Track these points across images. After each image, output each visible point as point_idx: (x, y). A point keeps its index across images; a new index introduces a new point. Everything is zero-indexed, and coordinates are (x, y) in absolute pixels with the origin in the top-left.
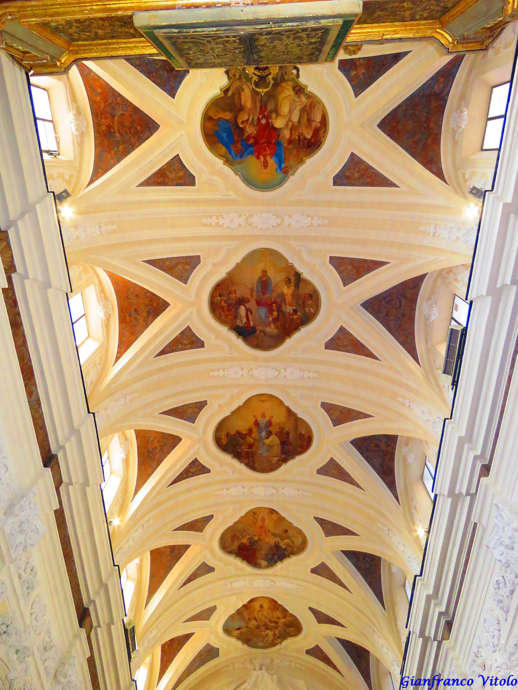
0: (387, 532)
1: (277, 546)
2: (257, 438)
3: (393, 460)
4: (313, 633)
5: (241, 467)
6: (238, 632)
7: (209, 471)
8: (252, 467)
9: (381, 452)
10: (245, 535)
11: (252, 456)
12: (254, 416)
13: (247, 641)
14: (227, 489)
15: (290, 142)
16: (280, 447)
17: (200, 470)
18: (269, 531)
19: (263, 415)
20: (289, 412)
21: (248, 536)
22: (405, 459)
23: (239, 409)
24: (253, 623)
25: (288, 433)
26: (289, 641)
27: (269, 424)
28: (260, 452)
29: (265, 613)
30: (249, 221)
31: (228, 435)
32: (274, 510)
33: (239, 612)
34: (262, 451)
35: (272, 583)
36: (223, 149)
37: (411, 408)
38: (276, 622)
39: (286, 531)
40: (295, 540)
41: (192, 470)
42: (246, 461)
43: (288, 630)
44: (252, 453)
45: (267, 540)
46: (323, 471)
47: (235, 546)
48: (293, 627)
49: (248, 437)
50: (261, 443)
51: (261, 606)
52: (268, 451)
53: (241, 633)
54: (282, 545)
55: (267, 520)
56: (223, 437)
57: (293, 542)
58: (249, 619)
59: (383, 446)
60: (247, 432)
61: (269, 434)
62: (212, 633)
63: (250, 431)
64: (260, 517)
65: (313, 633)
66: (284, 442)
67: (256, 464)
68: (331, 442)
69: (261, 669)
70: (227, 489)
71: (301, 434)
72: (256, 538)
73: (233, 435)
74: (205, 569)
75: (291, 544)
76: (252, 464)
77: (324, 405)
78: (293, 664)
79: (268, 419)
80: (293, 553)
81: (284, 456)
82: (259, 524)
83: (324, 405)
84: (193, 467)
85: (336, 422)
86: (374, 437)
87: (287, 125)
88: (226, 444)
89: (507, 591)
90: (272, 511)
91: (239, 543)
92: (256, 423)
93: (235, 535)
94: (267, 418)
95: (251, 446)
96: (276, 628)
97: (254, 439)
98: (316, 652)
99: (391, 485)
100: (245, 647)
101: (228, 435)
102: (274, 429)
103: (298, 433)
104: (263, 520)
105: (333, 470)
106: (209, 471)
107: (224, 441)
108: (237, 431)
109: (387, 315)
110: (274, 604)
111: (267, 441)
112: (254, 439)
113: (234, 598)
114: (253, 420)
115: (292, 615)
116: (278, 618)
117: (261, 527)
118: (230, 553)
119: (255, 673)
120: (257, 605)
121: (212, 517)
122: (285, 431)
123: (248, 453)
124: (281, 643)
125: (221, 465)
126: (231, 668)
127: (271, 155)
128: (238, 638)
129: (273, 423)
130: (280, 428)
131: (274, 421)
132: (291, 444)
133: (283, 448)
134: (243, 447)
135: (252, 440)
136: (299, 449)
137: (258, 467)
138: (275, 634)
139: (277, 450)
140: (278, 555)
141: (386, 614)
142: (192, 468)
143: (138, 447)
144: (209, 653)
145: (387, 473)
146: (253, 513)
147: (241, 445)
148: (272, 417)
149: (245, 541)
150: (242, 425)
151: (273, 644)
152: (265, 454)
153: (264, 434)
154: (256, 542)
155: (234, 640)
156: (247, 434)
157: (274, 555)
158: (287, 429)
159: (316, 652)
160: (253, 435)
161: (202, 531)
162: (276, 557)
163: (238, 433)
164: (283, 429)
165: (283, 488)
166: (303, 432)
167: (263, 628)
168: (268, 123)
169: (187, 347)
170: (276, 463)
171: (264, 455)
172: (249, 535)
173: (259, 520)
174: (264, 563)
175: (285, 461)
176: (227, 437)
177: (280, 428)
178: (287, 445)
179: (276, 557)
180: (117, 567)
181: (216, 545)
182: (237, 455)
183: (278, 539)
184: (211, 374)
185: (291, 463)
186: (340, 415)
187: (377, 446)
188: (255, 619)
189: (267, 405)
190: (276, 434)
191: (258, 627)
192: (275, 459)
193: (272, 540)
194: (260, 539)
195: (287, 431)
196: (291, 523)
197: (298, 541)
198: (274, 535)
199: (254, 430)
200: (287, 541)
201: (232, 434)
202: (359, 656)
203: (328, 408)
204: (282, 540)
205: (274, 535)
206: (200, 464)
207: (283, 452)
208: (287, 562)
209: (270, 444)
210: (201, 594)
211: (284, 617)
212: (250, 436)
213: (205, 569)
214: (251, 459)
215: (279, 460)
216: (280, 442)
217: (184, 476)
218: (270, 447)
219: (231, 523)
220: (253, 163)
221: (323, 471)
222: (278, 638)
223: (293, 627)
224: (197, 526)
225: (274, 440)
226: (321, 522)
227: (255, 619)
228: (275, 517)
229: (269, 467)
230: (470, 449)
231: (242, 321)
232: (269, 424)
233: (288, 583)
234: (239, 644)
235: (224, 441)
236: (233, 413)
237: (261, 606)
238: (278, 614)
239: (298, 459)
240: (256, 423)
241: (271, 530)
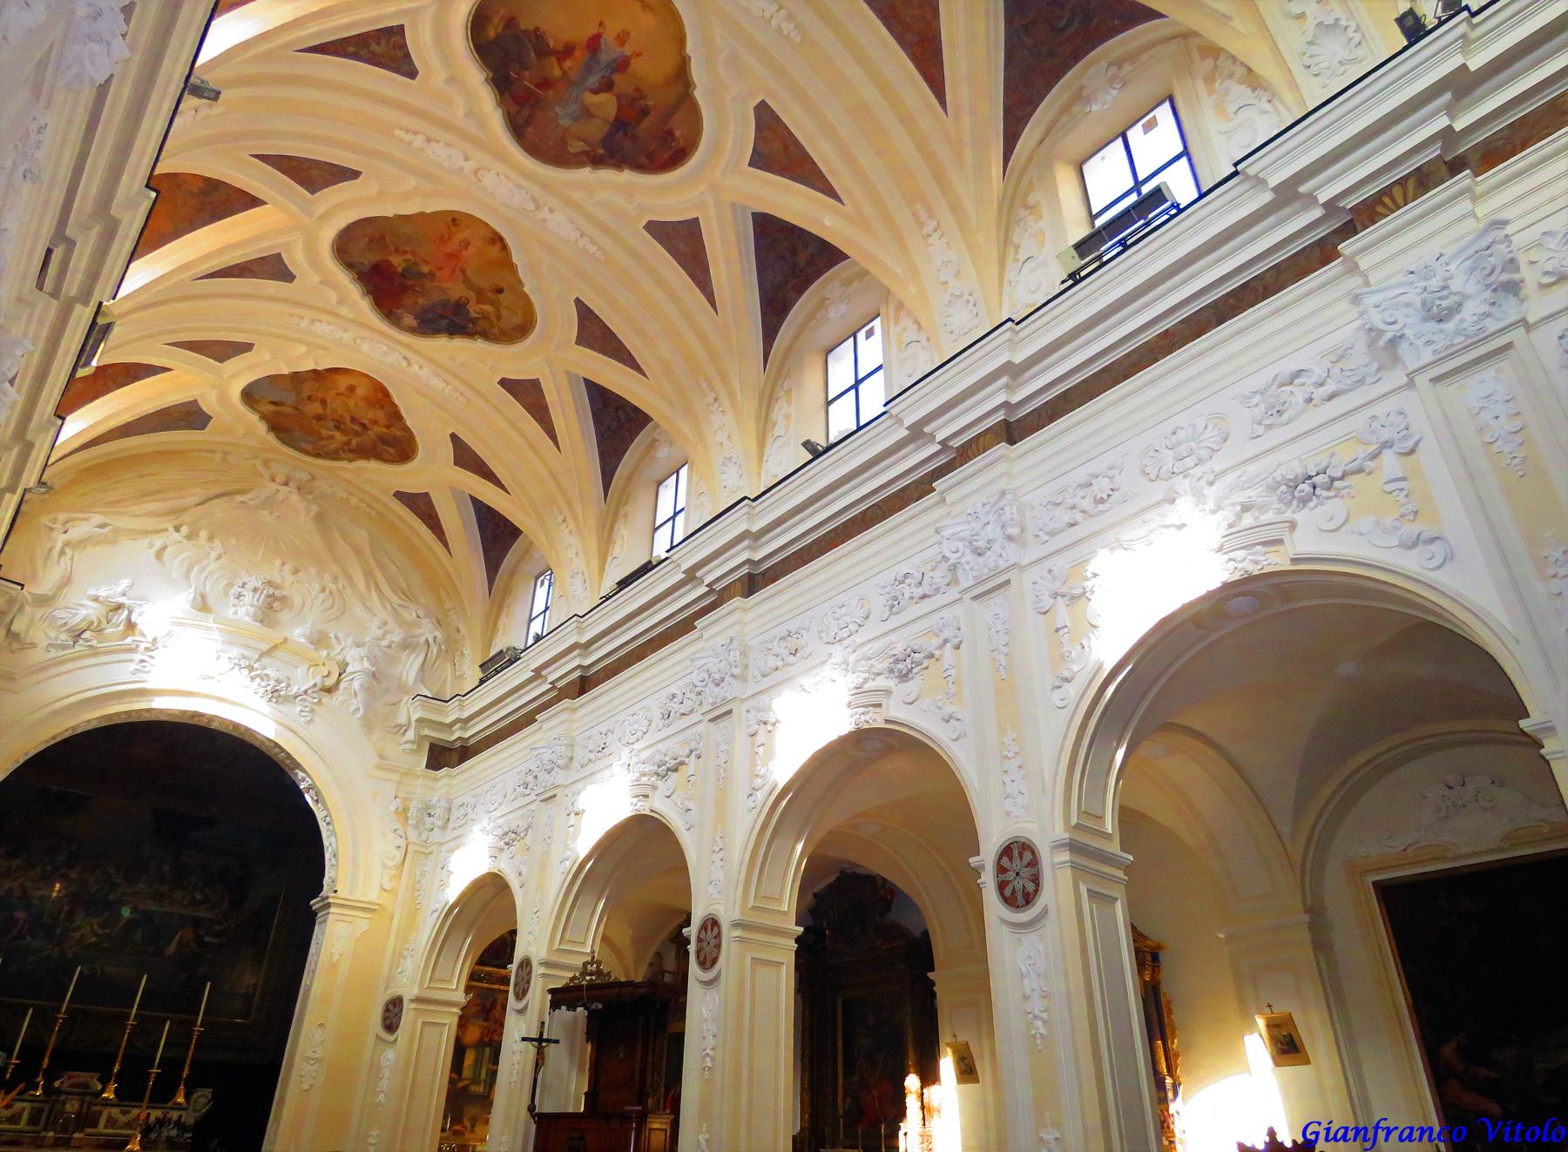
0: (711, 400)
1: (460, 306)
2: (573, 75)
3: (800, 291)
4: (431, 470)
6: (272, 408)
7: (412, 73)
8: (518, 129)
9: (792, 265)
12: (601, 24)
13: (277, 426)
14: (429, 140)
16: (607, 127)
18: (463, 271)
19: (622, 38)
20: (681, 75)
21: (409, 257)
22: (822, 304)
24: (316, 408)
25: (645, 112)
26: (373, 465)
27: (622, 65)
28: (558, 110)
29: (352, 403)
31: (511, 23)
32: (501, 239)
33: (296, 377)
34: (563, 115)
35: (404, 363)
37: (931, 240)
38: (363, 425)
39: (500, 291)
40: (505, 313)
41: (374, 47)
42: (514, 109)
43: (381, 447)
45: (445, 285)
46: (660, 231)
47: (368, 259)
48: (399, 447)
49: (554, 60)
51: (352, 389)
52: (576, 119)
53: (276, 413)
54: (474, 310)
56: (496, 20)
57: (499, 317)
58: (309, 398)
59: (802, 259)
60: (560, 48)
61: (607, 86)
62: (220, 387)
63: (567, 51)
64: (461, 236)
65: (431, 470)
66: (622, 125)
67: (530, 129)
68: (720, 186)
69: (286, 484)
70: (429, 140)
71: (670, 133)
72: (425, 269)
73: (524, 32)
74: (273, 268)
75: (494, 319)
77: (762, 109)
78: (354, 501)
80: (486, 336)
81: (601, 151)
82: (452, 246)
83: (762, 109)
84: (383, 42)
85: (761, 160)
86: (801, 233)
89: (919, 592)
90: (497, 240)
91: (379, 257)
92: (594, 43)
93: (382, 237)
94: (627, 50)
95: (545, 84)
96: (357, 434)
97: (565, 72)
98: (421, 505)
99: (770, 334)
100: (272, 439)
102: (622, 83)
103: (667, 128)
104: (466, 244)
105: (683, 241)
106: (412, 73)
107: (492, 32)
108: (537, 29)
109: (1026, 28)
110: (381, 396)
112: (565, 72)
113: (302, 349)
114: (592, 30)
115: (408, 430)
116: (375, 422)
117: (451, 256)
118: (349, 265)
119: (274, 486)
120: (343, 382)
121: (355, 174)
124: (351, 461)
125: (452, 80)
126: (218, 457)
128: (263, 417)
129: (629, 71)
130: (638, 90)
131: (635, 64)
132: (634, 138)
133: (611, 134)
134: (527, 74)
135: (557, 72)
136: (644, 160)
138: (348, 443)
139: (596, 129)
140: (450, 320)
141: (604, 507)
142: (378, 44)
144: (190, 416)
145: (775, 309)
146: (455, 220)
147: (525, 67)
148: (639, 55)
149: (397, 262)
151: (333, 455)
152: (565, 122)
153: (593, 80)
154: (422, 275)
155: (254, 418)
156: (553, 52)
157: (442, 317)
158: (650, 103)
159: (421, 505)
160: (568, 64)
161: (312, 192)
162: (444, 322)
163: (538, 36)
164: (643, 97)
165: (551, 211)
166: (678, 133)
167: (331, 425)
170: (576, 155)
172: (414, 253)
174: (409, 320)
175: (597, 162)
178: (626, 135)
179: (444, 322)
180: (154, 194)
181: (329, 234)
182: (501, 83)
183: (472, 295)
185: (608, 175)
186: (778, 150)
187: (794, 251)
188: (324, 402)
189: (648, 20)
190: (619, 97)
191: (319, 418)
192: (576, 146)
193: (456, 291)
194: (432, 275)
195: (647, 107)
196: (520, 282)
197: (511, 319)
198: (467, 282)
199: (578, 53)
200: (488, 308)
201: (523, 26)
202: (498, 535)
203: (767, 120)
204: (479, 302)
205: (467, 282)
206: (403, 46)
207: (607, 142)
208: (459, 344)
210: (229, 311)
211: (388, 427)
212: (560, 60)
213: (273, 268)
214: (526, 113)
215: (585, 153)
217: (351, 49)
218: (587, 113)
219: (389, 210)
221: (660, 231)
222: (351, 451)
223: (399, 447)
224: (311, 175)
225: (606, 104)
226: (586, 315)
227: (324, 402)
228: (495, 251)
229: (552, 151)
230: (1007, 386)
232: (622, 65)
233: (436, 380)
234: (262, 428)
235: (492, 32)
237: (352, 389)
238: (380, 415)
239: (627, 176)
240: (594, 43)
241: (470, 273)
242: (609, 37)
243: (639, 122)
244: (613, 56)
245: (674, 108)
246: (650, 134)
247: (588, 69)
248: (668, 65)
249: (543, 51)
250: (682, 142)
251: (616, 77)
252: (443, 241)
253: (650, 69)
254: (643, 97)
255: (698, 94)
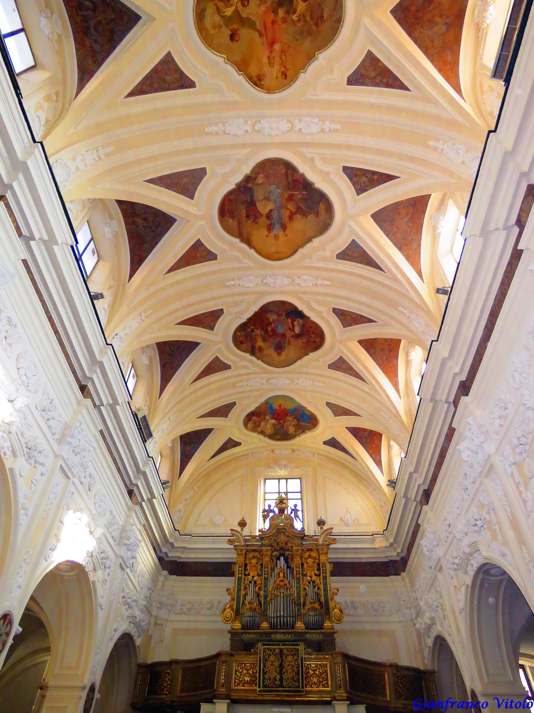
5: (303, 168)
7: (346, 169)
8: (289, 167)
9: (143, 227)
10: (299, 20)
11: (289, 183)
12: (287, 235)
15: (265, 415)
16: (255, 198)
17: (356, 175)
19: (276, 237)
20: (249, 243)
21: (295, 17)
23: (302, 246)
25: (248, 216)
27: (270, 228)
28: (279, 191)
30: (290, 125)
31: (317, 214)
34: (277, 191)
36: (306, 412)
39: (233, 37)
42: (296, 177)
44: (289, 189)
49: (294, 210)
50: (278, 204)
55: (265, 60)
56: (323, 212)
60: (294, 216)
61: (269, 216)
63: (291, 218)
67: (283, 171)
71: (233, 218)
73: (310, 214)
76: (289, 172)
79: (271, 234)
81: (250, 185)
84: (363, 184)
87: (268, 421)
88: (319, 202)
92: (284, 227)
94: (272, 234)
95: (290, 198)
97: (287, 208)
101: (317, 214)
103: (236, 218)
106: (346, 169)
108: (307, 218)
111: (270, 206)
112: (287, 208)
114: (288, 231)
122: (252, 219)
123: (294, 189)
127: (276, 410)
129: (266, 228)
130: (257, 223)
131: (265, 232)
132: (243, 203)
133: (252, 197)
134: (300, 197)
136: (232, 197)
137: (282, 166)
139: (259, 194)
142: (364, 182)
143: (424, 212)
148: (267, 236)
150: (299, 224)
153: (275, 215)
156: (295, 213)
160: (288, 213)
163: (304, 215)
164: (254, 222)
166: (231, 220)
168: (279, 421)
169: (348, 313)
170: (258, 174)
171: (274, 186)
173: (277, 60)
175: (248, 179)
176: (318, 212)
177: (257, 223)
178: (247, 201)
182: (306, 185)
184: (329, 283)
187: (145, 219)
189: (273, 249)
190: (261, 215)
192: (260, 179)
195: (249, 220)
199: (287, 220)
201: (312, 215)
206: (354, 184)
209: (267, 202)
214: (290, 178)
215: (255, 179)
216: (255, 205)
218: (267, 199)
220: (289, 406)
225: (264, 208)
231: (298, 323)
232: (270, 228)
235: (322, 207)
236: (310, 240)
240: (284, 227)
242: (281, 233)
243: (247, 211)
244: (275, 230)
245: (239, 228)
246: (240, 209)
247: (280, 218)
248: (255, 240)
249: (299, 210)
250: (226, 219)
251: (268, 222)
252: (282, 52)
253: (259, 234)
254: (254, 222)
255: (237, 241)
